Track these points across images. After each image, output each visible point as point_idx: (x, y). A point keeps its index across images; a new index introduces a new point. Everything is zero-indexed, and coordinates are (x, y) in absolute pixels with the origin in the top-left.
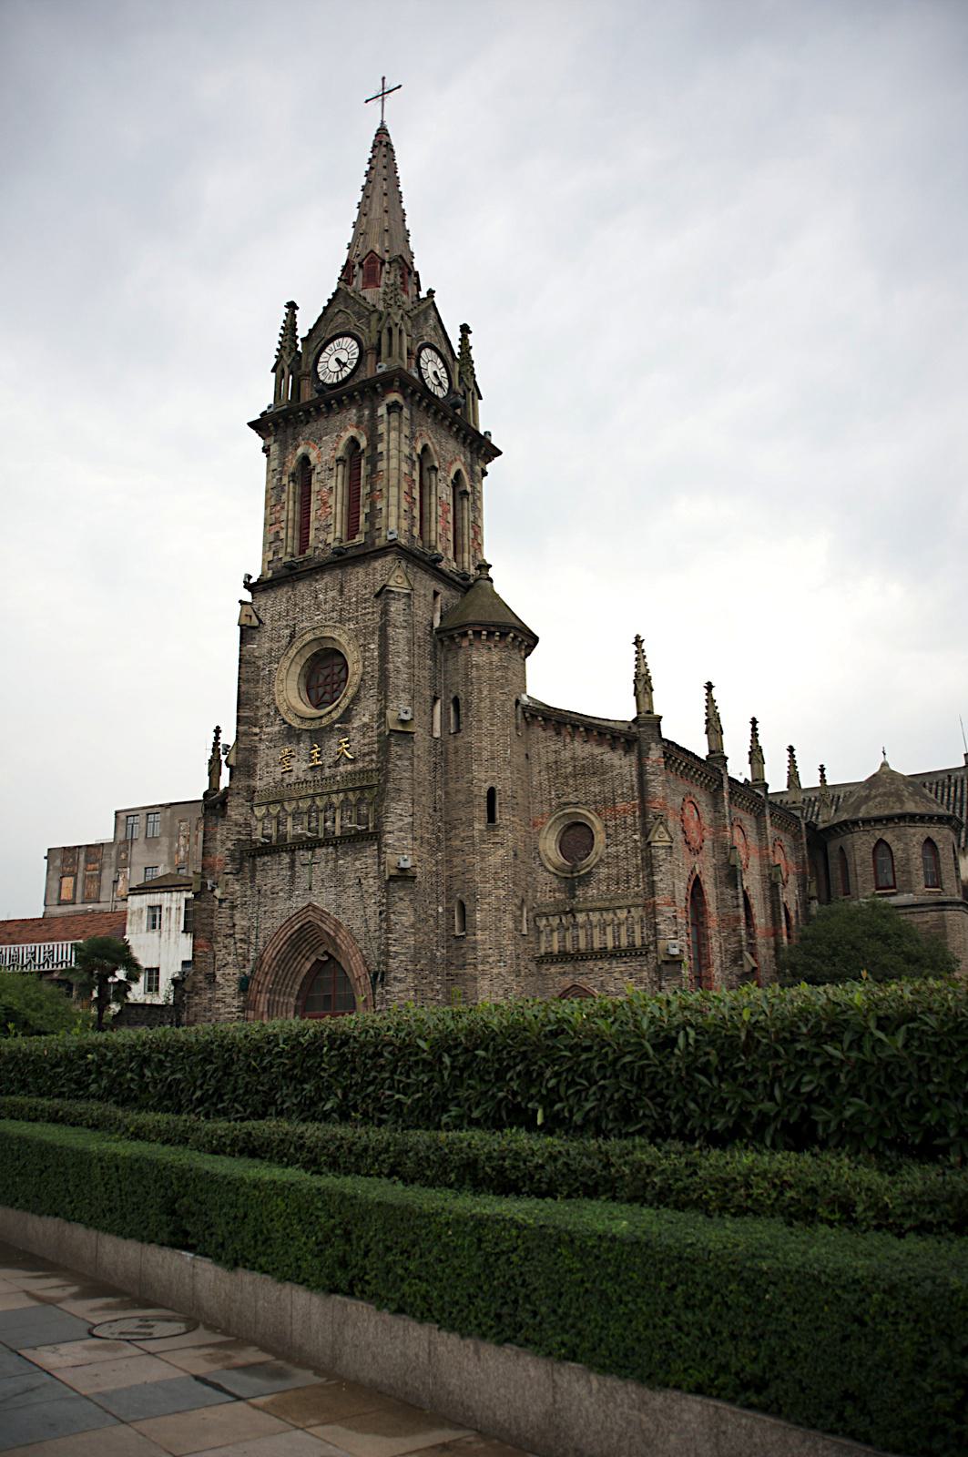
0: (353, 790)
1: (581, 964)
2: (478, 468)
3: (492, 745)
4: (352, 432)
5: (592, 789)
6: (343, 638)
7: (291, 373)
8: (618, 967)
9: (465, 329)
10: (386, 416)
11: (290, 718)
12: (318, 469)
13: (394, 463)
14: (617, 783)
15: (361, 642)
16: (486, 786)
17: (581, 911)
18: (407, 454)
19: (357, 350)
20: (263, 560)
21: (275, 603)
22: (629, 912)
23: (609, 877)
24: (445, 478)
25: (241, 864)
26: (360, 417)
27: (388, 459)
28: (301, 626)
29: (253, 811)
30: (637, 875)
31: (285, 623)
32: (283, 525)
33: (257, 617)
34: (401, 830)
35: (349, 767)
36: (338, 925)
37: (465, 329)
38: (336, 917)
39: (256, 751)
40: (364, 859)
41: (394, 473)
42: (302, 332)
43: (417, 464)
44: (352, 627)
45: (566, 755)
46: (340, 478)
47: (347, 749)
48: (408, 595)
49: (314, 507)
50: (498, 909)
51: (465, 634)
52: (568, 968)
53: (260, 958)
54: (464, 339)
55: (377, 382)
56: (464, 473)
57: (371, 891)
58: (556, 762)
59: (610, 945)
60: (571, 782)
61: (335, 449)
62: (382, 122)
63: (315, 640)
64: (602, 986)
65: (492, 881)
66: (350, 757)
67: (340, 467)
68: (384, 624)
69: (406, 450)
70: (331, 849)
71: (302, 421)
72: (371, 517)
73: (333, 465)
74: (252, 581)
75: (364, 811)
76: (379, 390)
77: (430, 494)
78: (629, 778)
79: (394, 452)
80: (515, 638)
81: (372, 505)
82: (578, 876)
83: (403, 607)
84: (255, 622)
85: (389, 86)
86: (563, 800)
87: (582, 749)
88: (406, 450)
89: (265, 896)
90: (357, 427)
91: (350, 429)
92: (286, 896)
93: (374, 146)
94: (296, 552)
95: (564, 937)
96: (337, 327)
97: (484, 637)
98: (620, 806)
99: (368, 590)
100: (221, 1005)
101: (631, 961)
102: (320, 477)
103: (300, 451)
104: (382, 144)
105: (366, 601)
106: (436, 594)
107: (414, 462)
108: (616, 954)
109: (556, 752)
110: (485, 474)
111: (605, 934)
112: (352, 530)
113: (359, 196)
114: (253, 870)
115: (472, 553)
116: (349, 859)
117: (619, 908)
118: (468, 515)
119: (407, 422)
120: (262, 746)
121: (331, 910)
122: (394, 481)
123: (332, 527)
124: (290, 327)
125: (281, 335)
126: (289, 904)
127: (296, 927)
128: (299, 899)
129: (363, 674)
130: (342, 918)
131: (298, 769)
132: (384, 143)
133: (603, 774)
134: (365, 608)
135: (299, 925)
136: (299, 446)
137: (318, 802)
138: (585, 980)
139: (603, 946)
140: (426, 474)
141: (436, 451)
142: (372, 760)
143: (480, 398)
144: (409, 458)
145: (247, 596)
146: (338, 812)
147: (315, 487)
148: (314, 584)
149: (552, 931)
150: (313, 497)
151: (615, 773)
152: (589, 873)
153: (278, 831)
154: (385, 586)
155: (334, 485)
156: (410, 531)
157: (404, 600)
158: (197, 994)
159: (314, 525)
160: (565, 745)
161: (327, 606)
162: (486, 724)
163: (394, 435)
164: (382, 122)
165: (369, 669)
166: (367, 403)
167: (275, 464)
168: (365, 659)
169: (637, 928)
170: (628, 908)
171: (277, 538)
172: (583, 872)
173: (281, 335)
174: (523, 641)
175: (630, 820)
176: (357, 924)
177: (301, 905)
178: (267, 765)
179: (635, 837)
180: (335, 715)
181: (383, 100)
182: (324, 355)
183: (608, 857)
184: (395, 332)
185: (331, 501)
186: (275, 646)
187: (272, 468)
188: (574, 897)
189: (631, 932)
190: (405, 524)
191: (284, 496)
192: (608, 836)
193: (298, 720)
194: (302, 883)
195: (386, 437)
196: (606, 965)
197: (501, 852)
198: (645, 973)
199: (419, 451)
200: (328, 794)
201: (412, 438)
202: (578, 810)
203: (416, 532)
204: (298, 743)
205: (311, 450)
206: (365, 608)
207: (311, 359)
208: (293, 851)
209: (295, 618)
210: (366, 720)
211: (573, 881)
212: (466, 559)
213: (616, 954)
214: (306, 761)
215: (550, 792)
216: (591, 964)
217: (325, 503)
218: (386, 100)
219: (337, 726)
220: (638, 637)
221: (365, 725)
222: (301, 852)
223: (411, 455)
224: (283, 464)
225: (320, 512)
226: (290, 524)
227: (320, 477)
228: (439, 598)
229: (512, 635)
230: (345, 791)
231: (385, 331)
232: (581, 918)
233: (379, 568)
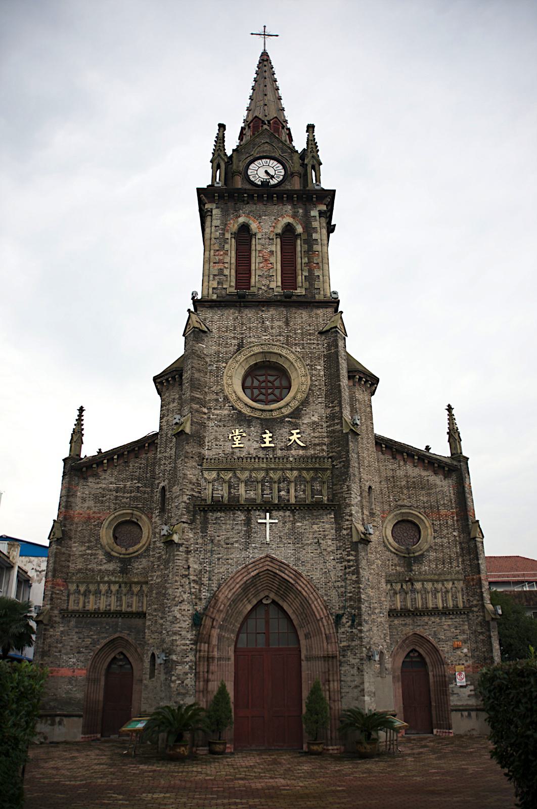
0: (308, 470)
1: (418, 618)
3: (369, 457)
5: (421, 498)
6: (290, 356)
8: (447, 622)
10: (318, 217)
11: (239, 406)
12: (259, 236)
14: (440, 496)
15: (308, 362)
16: (368, 484)
17: (418, 581)
21: (218, 320)
22: (453, 584)
23: (437, 559)
25: (194, 516)
28: (249, 340)
29: (202, 474)
30: (457, 560)
31: (232, 335)
32: (226, 265)
35: (301, 452)
36: (298, 575)
38: (296, 568)
39: (205, 427)
40: (321, 524)
44: (299, 350)
45: (400, 473)
47: (298, 438)
50: (378, 574)
52: (408, 621)
53: (214, 597)
55: (315, 194)
57: (329, 549)
58: (393, 477)
59: (440, 606)
60: (405, 492)
62: (265, 50)
63: (262, 352)
64: (435, 634)
65: (374, 553)
66: (302, 444)
70: (288, 513)
71: (243, 201)
74: (199, 297)
75: (317, 487)
78: (448, 494)
81: (311, 271)
82: (414, 557)
86: (400, 503)
87: (413, 471)
89: (219, 545)
92: (241, 547)
95: (405, 598)
98: (443, 512)
99: (312, 328)
100: (177, 637)
101: (456, 618)
102: (262, 241)
103: (241, 220)
105: (310, 334)
108: (445, 612)
109: (393, 470)
111: (436, 598)
114: (205, 523)
116: (305, 522)
117: (446, 580)
120: (211, 424)
121: (291, 562)
124: (220, 140)
126: (244, 554)
127: (252, 574)
128: (256, 551)
129: (311, 385)
130: (301, 569)
131: (249, 447)
133: (429, 489)
134: (310, 340)
135: (257, 571)
136: (240, 217)
137: (271, 474)
138: (422, 630)
139: (434, 606)
142: (323, 450)
146: (293, 485)
148: (261, 313)
149: (395, 593)
151: (437, 490)
152: (422, 555)
153: (230, 493)
158: (52, 627)
160: (399, 466)
161: (274, 331)
162: (365, 441)
164: (265, 50)
165: (317, 383)
168: (312, 376)
169: (460, 595)
170: (453, 581)
172: (417, 554)
175: (450, 522)
176: (316, 575)
177: (258, 556)
178: (216, 439)
179: (455, 533)
180: (286, 411)
183: (435, 545)
185: (272, 260)
186: (223, 350)
188: (411, 571)
189: (455, 598)
191: (227, 247)
192: (435, 531)
193: (249, 410)
194: (257, 538)
196: (437, 620)
198: (466, 627)
200: (282, 469)
202: (411, 511)
204: (249, 427)
206: (310, 340)
208: (249, 511)
209: (242, 334)
210: (315, 419)
211: (409, 559)
213: (445, 612)
214: (257, 442)
215: (389, 497)
216: (426, 619)
219: (287, 419)
220: (449, 406)
221: (314, 423)
222: (258, 513)
225: (261, 265)
230: (299, 470)
232: (418, 586)
233: (321, 315)
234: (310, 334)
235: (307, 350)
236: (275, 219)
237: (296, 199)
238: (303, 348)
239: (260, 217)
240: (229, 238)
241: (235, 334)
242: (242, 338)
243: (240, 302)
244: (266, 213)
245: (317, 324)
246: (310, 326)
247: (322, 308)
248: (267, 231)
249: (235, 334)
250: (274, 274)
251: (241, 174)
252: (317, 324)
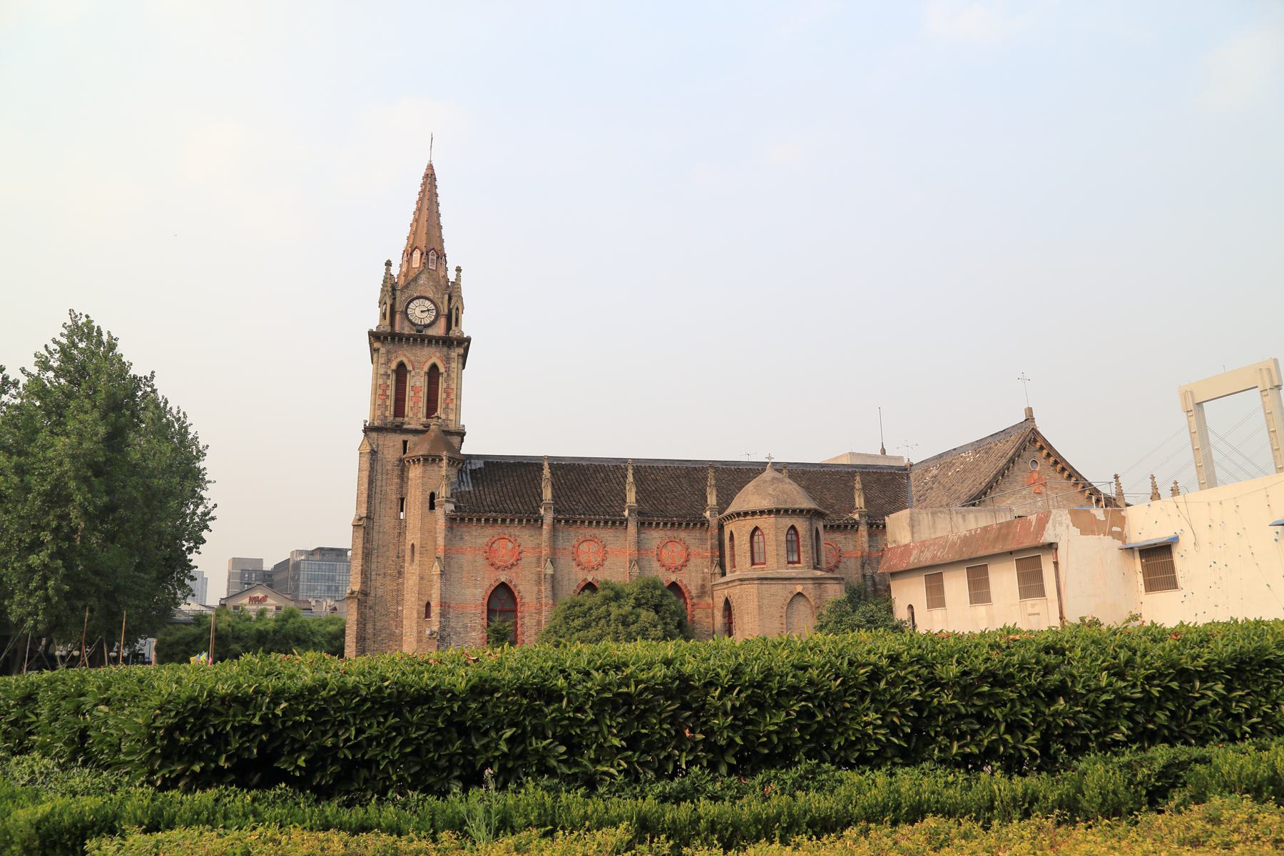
9: (459, 270)
18: (383, 372)
34: (356, 574)
37: (459, 270)
43: (393, 377)
104: (430, 177)
118: (442, 385)
156: (383, 414)
197: (414, 577)
201: (389, 361)
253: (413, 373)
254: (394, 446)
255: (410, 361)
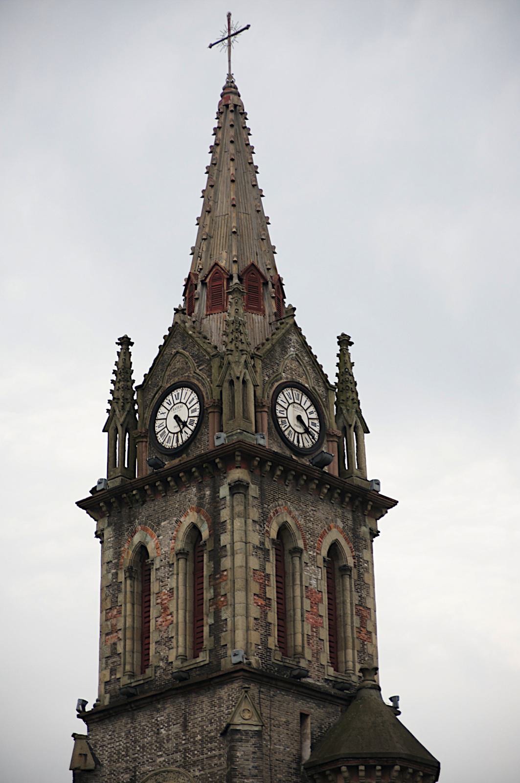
2: (364, 530)
4: (191, 517)
7: (127, 431)
9: (344, 341)
10: (228, 498)
12: (157, 564)
13: (239, 560)
18: (257, 543)
19: (197, 406)
20: (100, 680)
24: (313, 559)
26: (201, 498)
27: (233, 554)
31: (124, 765)
32: (120, 635)
33: (93, 755)
37: (344, 341)
41: (240, 574)
42: (138, 378)
43: (272, 557)
44: (197, 773)
46: (181, 576)
48: (259, 734)
49: (154, 612)
51: (338, 771)
54: (343, 355)
56: (343, 542)
61: (174, 538)
62: (230, 76)
67: (181, 562)
68: (229, 773)
69: (255, 539)
71: (137, 501)
72: (218, 628)
73: (172, 559)
74: (89, 708)
76: (220, 466)
77: (294, 584)
79: (238, 546)
80: (403, 770)
83: (252, 749)
84: (91, 763)
85: (237, 25)
88: (255, 539)
90: (198, 512)
91: (191, 513)
93: (220, 113)
94: (137, 670)
96: (175, 374)
97: (362, 774)
102: (161, 574)
103: (137, 539)
105: (212, 740)
106: (303, 717)
107: (267, 551)
110: (375, 533)
112: (197, 646)
113: (202, 181)
115: (358, 646)
118: (350, 598)
119: (256, 502)
122: (240, 583)
123: (174, 640)
124: (124, 370)
125: (113, 382)
132: (231, 108)
134: (211, 750)
136: (135, 533)
140: (288, 558)
141: (299, 528)
143: (367, 431)
144: (261, 549)
145: (82, 728)
147: (155, 587)
150: (153, 598)
154: (229, 725)
155: (174, 585)
156: (264, 643)
157: (253, 741)
159: (154, 637)
163: (238, 523)
164: (230, 76)
166: (208, 480)
167: (110, 553)
171: (114, 653)
173: (113, 382)
174: (415, 772)
181: (229, 45)
182: (162, 409)
184: (238, 385)
185: (172, 607)
187: (107, 560)
190: (255, 637)
191: (121, 598)
195: (229, 527)
199: (274, 534)
201: (265, 519)
203: (273, 642)
205: (149, 538)
206: (211, 750)
207: (148, 414)
209: (135, 760)
212: (350, 657)
217: (166, 609)
218: (233, 45)
223: (263, 543)
224: (118, 555)
225: (160, 620)
226: (129, 634)
227: (161, 574)
228: (309, 721)
229: (397, 768)
231: (226, 385)
234: (211, 738)
235: (207, 771)
236: (177, 522)
237: (196, 474)
238: (203, 769)
239: (159, 524)
240: (123, 580)
241: (126, 762)
242: (134, 767)
243: (130, 703)
244: (167, 513)
245: (219, 718)
246: (211, 723)
247: (226, 684)
248: (167, 549)
249: (126, 762)
250: (173, 634)
251: (146, 437)
252: (219, 718)
253: (305, 557)
254: (287, 723)
255: (299, 528)
